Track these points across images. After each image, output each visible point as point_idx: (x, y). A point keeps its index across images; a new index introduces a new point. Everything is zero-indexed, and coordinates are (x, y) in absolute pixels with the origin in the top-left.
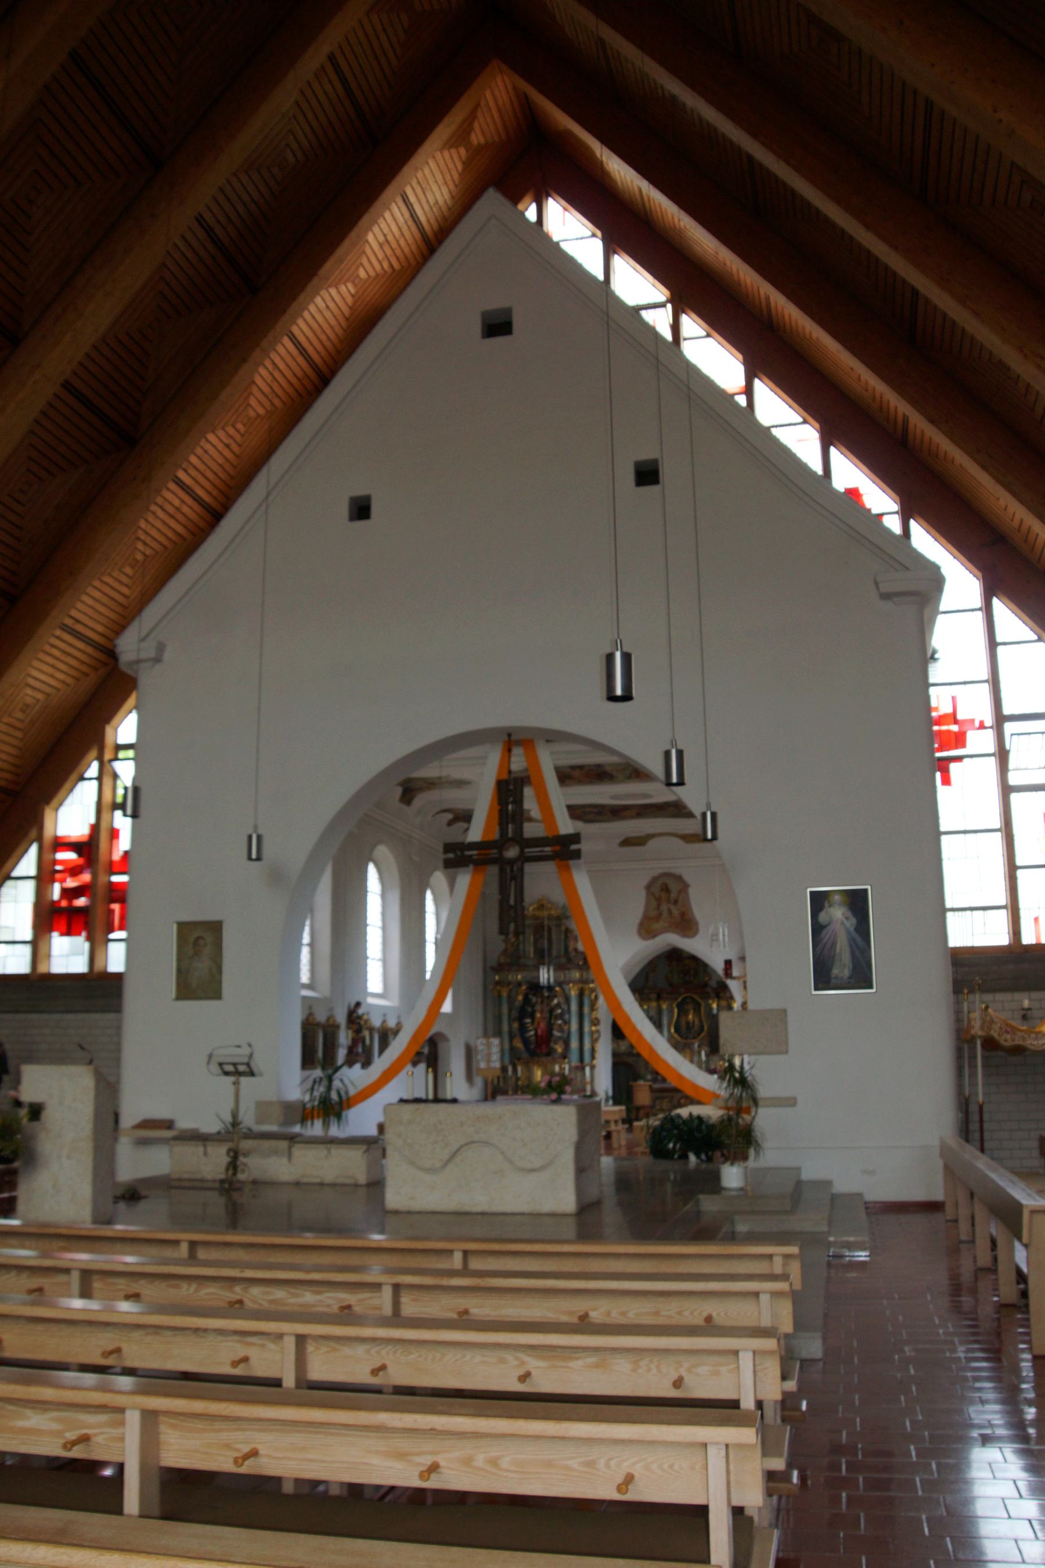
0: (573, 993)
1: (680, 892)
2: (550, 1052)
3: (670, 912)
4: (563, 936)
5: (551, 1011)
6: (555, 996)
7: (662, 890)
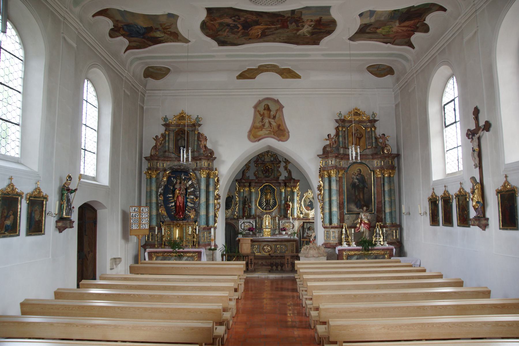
0: (203, 176)
1: (277, 110)
2: (186, 218)
3: (270, 123)
5: (186, 189)
6: (190, 179)
7: (265, 109)
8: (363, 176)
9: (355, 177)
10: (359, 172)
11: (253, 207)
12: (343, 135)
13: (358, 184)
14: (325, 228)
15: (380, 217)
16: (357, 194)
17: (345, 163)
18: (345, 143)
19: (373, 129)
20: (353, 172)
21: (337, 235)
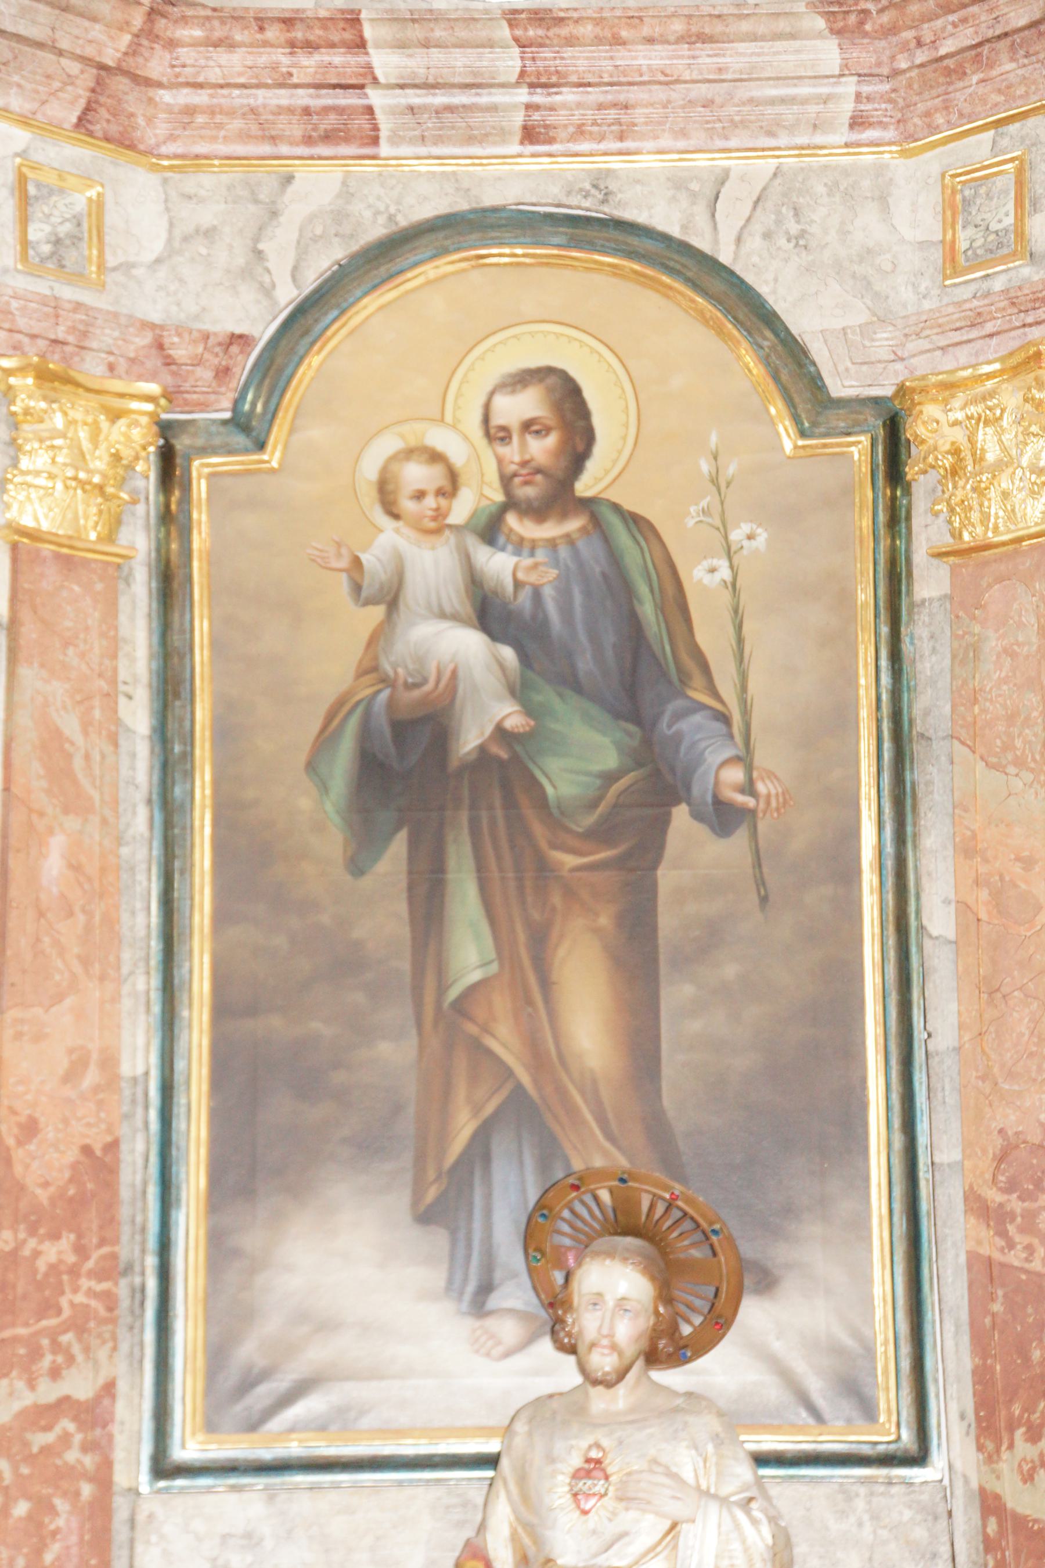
8: (636, 522)
17: (209, 233)
20: (388, 445)
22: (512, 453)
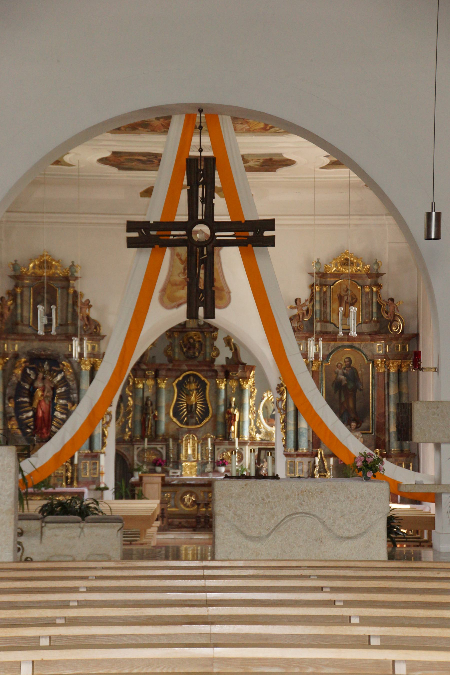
4: (70, 302)
8: (355, 369)
9: (340, 371)
10: (348, 363)
11: (163, 418)
12: (322, 299)
13: (346, 382)
14: (287, 455)
15: (381, 439)
16: (343, 399)
17: (325, 347)
18: (325, 312)
19: (375, 289)
21: (306, 468)
22: (346, 363)
